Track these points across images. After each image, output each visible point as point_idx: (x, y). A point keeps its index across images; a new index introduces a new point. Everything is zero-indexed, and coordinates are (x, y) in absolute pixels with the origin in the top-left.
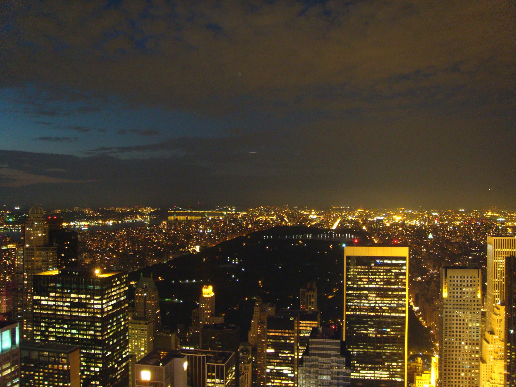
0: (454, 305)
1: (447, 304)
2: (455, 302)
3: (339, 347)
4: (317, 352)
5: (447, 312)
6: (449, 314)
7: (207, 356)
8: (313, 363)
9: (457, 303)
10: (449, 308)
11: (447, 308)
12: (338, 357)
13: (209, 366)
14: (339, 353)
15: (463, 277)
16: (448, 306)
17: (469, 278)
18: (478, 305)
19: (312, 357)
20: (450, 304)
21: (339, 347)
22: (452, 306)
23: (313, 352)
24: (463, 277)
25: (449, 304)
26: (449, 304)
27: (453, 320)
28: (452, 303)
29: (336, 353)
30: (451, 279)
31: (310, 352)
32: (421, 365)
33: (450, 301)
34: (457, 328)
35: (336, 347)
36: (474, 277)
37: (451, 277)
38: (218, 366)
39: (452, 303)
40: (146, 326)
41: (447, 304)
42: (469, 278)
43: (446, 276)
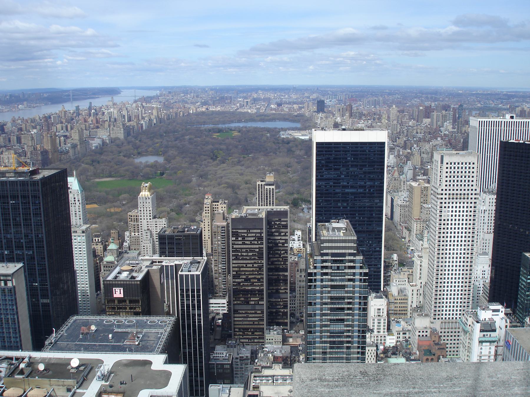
0: (449, 194)
1: (442, 194)
2: (451, 192)
3: (355, 245)
4: (330, 251)
5: (441, 203)
6: (444, 205)
7: (175, 265)
8: (325, 264)
9: (453, 192)
10: (444, 199)
11: (442, 199)
12: (355, 256)
13: (181, 276)
14: (355, 252)
15: (460, 163)
16: (444, 196)
17: (468, 164)
18: (475, 194)
19: (325, 258)
20: (446, 194)
21: (355, 245)
22: (447, 196)
23: (325, 251)
24: (460, 163)
25: (444, 194)
26: (444, 194)
27: (448, 211)
28: (448, 192)
29: (352, 251)
30: (447, 166)
31: (322, 252)
32: (397, 262)
33: (446, 190)
34: (452, 220)
35: (352, 245)
36: (473, 164)
37: (447, 164)
38: (192, 276)
39: (448, 192)
40: (84, 234)
41: (442, 194)
42: (468, 164)
43: (442, 162)
